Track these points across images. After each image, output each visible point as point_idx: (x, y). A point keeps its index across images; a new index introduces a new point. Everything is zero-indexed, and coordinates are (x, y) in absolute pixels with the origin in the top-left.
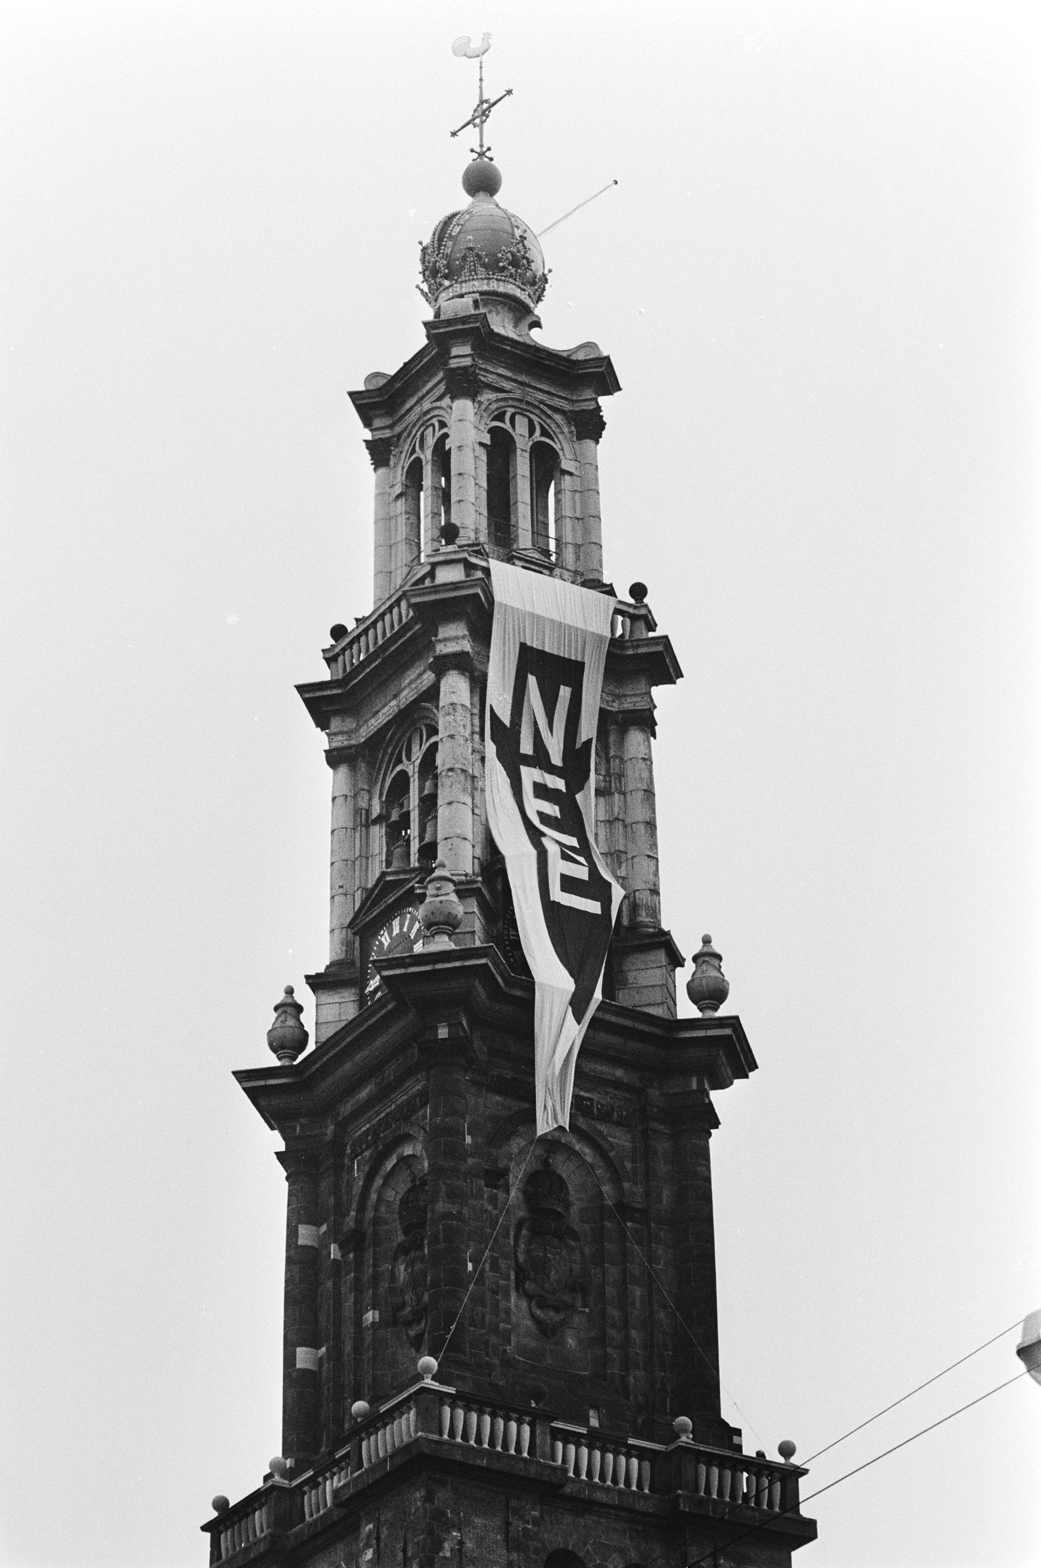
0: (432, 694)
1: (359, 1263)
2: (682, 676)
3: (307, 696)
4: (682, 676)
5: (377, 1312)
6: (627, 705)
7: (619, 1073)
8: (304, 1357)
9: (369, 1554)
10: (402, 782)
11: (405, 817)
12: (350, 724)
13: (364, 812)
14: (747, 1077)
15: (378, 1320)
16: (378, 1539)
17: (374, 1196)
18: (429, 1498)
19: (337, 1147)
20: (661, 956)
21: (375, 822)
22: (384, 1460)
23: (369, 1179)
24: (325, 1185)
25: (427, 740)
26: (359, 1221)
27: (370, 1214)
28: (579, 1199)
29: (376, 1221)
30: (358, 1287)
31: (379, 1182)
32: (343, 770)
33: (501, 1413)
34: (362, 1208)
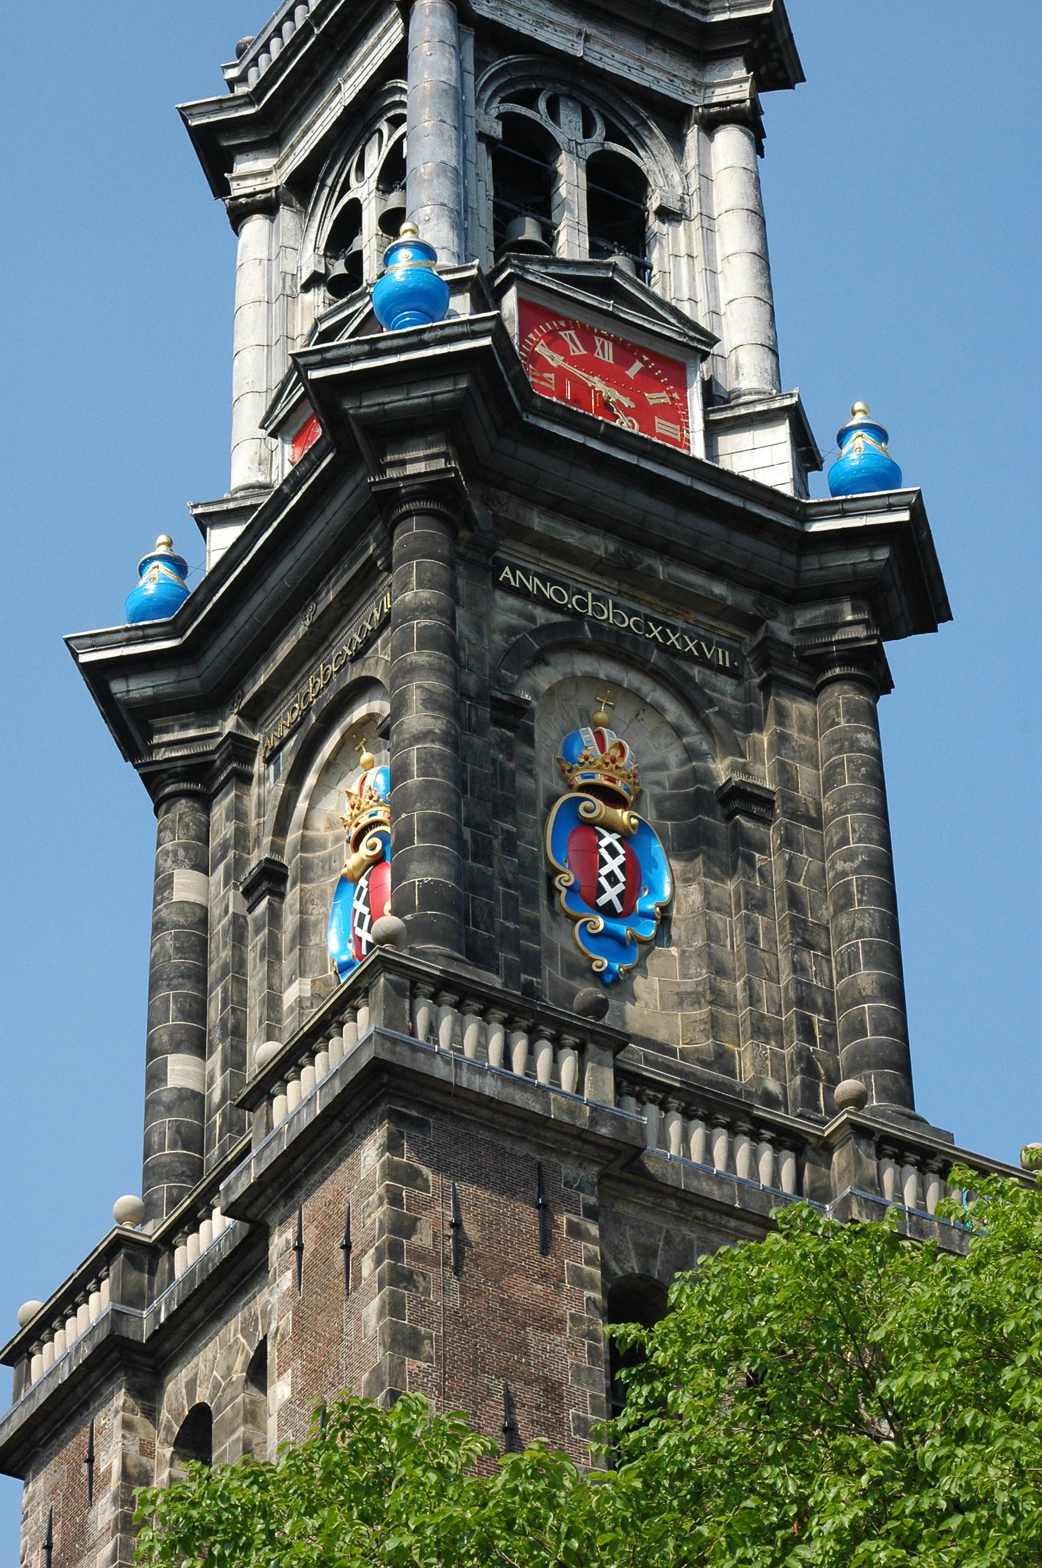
0: (397, 64)
1: (274, 916)
2: (803, 80)
3: (193, 123)
4: (803, 80)
5: (308, 981)
6: (720, 95)
7: (719, 589)
8: (181, 1071)
9: (286, 1281)
10: (349, 222)
11: (355, 262)
12: (264, 163)
13: (289, 278)
14: (935, 630)
15: (309, 995)
16: (299, 1249)
17: (302, 805)
18: (392, 1145)
19: (241, 750)
20: (782, 432)
21: (306, 287)
22: (310, 1101)
23: (296, 777)
24: (220, 810)
25: (390, 137)
26: (276, 848)
27: (293, 836)
28: (658, 783)
29: (305, 845)
30: (272, 951)
31: (311, 780)
32: (256, 226)
33: (524, 1023)
34: (281, 828)
